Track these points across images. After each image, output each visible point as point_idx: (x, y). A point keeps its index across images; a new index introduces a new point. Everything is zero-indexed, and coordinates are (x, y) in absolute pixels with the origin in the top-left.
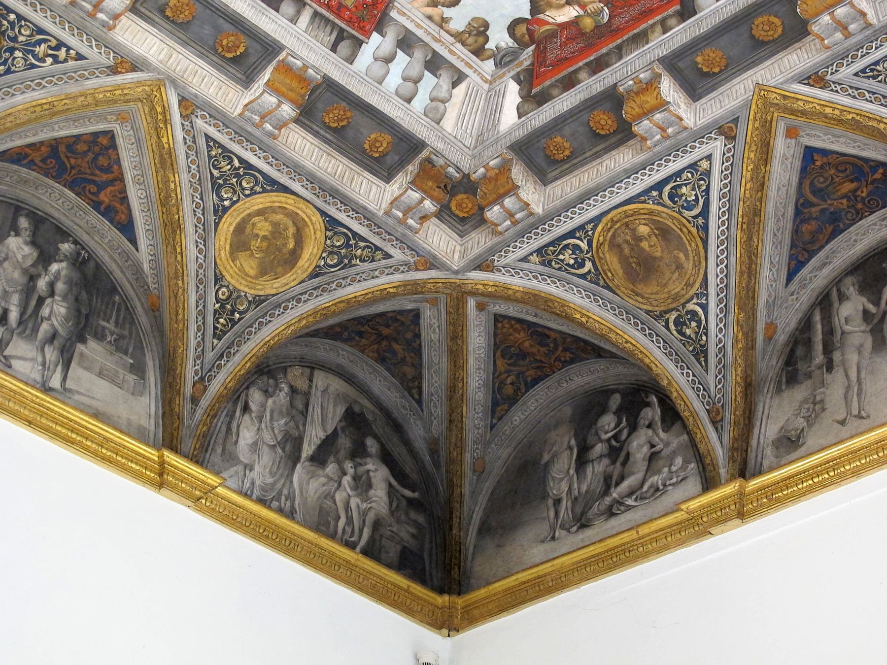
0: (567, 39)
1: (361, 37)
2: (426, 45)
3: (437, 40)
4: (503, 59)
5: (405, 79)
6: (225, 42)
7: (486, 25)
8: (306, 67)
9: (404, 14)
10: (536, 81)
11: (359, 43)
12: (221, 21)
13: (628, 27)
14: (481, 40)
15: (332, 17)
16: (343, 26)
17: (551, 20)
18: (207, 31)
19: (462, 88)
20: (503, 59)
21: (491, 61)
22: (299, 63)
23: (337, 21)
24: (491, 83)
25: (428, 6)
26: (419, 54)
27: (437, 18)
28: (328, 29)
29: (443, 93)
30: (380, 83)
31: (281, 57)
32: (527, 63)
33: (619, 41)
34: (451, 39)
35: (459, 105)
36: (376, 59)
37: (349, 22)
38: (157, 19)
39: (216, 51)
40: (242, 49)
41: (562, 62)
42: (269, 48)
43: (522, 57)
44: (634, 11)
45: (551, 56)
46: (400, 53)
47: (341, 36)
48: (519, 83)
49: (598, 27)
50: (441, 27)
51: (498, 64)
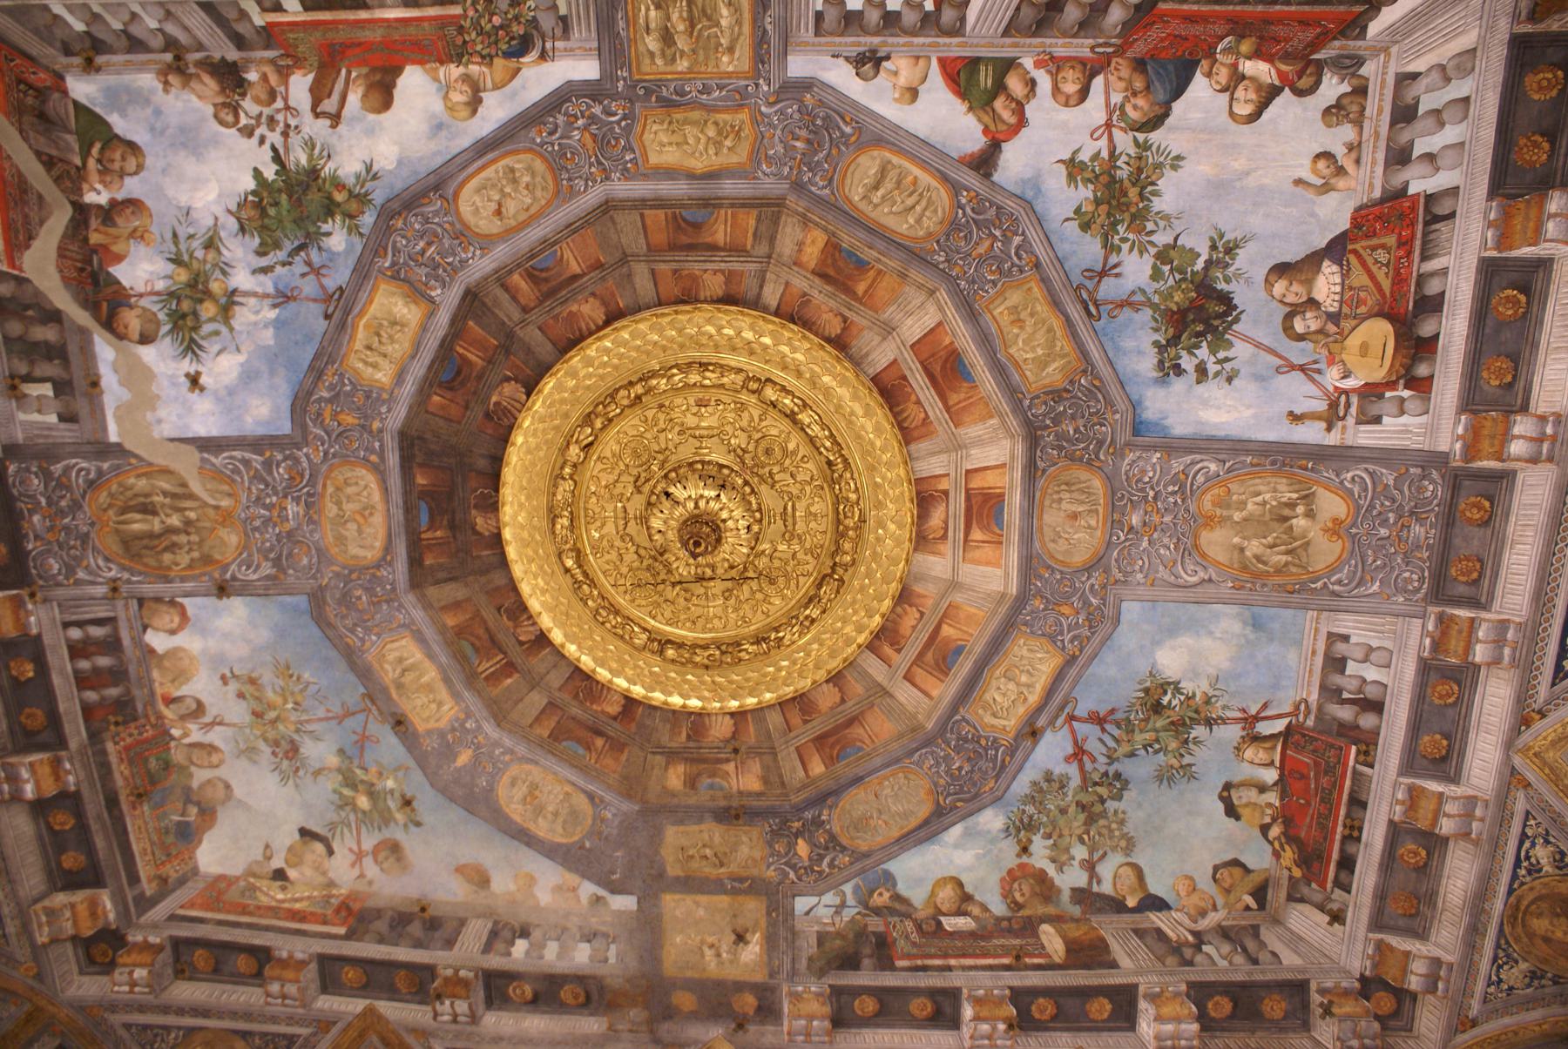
0: (1279, 42)
1: (1422, 200)
2: (1389, 139)
3: (1377, 134)
4: (1349, 65)
5: (1442, 124)
6: (1510, 312)
7: (1327, 112)
8: (1490, 225)
9: (1371, 185)
10: (1350, 18)
11: (1430, 198)
12: (1487, 331)
13: (1218, 16)
14: (1345, 101)
15: (1418, 243)
16: (1420, 226)
17: (1273, 71)
18: (1506, 335)
19: (1411, 68)
20: (1349, 65)
21: (1363, 71)
22: (1489, 234)
23: (1419, 235)
24: (1386, 50)
25: (1346, 173)
26: (1404, 138)
27: (1354, 155)
28: (1432, 237)
29: (1435, 76)
30: (1462, 144)
31: (1495, 254)
32: (1337, 43)
33: (1238, 8)
34: (1366, 124)
35: (1437, 52)
36: (1438, 170)
37: (1413, 224)
38: (1522, 384)
39: (1525, 314)
40: (1509, 292)
41: (1305, 22)
42: (1490, 272)
43: (1333, 53)
44: (1197, 30)
45: (1311, 34)
46: (1416, 153)
47: (1433, 219)
48: (1364, 29)
49: (1241, 37)
50: (1360, 144)
51: (1360, 62)
